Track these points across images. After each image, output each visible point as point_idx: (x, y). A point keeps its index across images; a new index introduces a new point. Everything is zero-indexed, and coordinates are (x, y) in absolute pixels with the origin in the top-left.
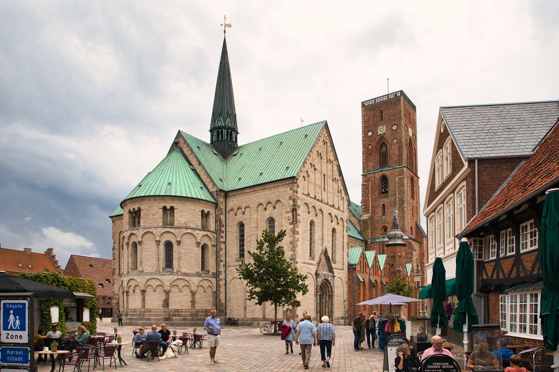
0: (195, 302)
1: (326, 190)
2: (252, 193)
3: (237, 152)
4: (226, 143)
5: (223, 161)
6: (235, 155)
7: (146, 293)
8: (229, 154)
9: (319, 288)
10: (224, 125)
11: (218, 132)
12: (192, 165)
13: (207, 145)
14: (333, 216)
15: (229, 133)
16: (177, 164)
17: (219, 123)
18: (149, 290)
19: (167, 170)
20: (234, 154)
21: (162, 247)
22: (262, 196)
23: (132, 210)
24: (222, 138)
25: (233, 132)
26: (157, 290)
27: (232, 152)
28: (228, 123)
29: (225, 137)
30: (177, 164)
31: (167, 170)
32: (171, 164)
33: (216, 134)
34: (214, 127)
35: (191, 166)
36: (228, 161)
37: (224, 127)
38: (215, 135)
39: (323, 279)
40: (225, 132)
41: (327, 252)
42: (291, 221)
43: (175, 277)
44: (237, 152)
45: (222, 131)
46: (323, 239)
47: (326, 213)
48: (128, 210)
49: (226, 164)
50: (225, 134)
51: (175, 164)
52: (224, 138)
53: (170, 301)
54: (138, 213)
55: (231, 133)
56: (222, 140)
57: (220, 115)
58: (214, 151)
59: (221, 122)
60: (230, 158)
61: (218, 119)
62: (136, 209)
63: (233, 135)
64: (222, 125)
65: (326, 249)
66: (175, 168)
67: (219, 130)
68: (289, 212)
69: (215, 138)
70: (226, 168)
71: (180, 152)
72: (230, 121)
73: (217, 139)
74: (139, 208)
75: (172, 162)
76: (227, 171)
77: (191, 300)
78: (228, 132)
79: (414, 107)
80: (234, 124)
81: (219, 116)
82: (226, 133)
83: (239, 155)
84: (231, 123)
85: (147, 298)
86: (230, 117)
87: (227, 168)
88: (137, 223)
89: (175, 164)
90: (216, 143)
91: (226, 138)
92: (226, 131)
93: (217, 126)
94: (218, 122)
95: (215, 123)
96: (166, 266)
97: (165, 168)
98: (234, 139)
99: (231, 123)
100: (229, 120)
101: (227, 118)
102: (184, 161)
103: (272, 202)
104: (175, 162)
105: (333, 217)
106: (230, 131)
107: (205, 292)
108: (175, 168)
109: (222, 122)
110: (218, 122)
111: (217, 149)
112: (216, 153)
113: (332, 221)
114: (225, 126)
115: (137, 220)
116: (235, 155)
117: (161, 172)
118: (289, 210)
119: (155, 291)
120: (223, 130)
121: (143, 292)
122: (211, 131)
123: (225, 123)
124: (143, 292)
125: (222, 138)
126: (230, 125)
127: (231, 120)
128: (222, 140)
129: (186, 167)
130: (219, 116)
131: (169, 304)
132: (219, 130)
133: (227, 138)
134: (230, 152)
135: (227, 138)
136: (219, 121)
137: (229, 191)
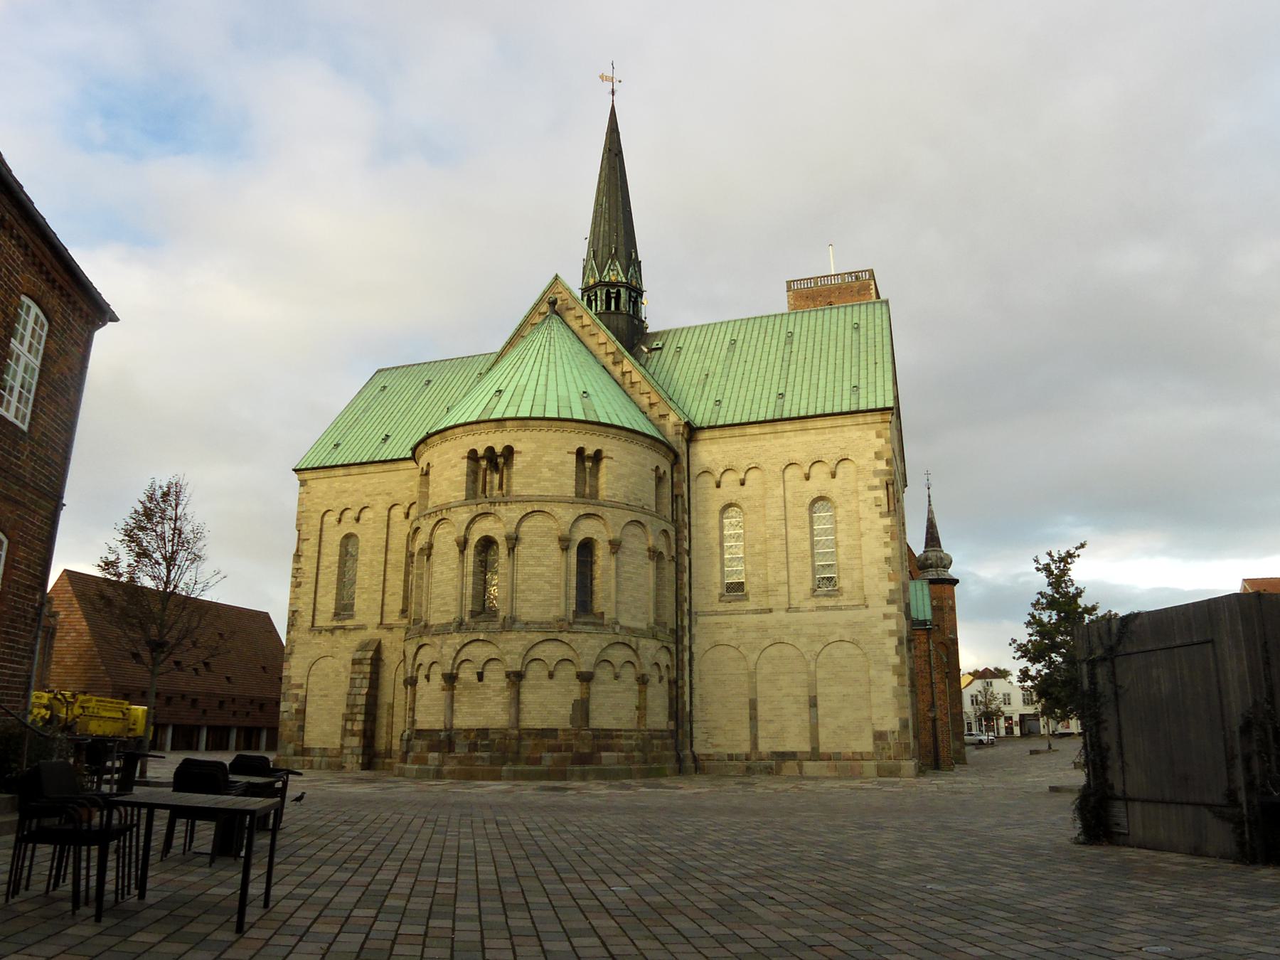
2: (768, 436)
7: (524, 682)
17: (611, 273)
18: (534, 671)
22: (797, 443)
26: (560, 674)
42: (885, 508)
53: (592, 707)
59: (615, 273)
64: (620, 279)
68: (876, 487)
85: (528, 696)
93: (607, 280)
94: (608, 272)
103: (827, 461)
109: (618, 273)
110: (608, 272)
118: (876, 482)
119: (551, 676)
120: (622, 290)
121: (516, 678)
124: (516, 678)
131: (591, 715)
132: (612, 291)
137: (702, 429)
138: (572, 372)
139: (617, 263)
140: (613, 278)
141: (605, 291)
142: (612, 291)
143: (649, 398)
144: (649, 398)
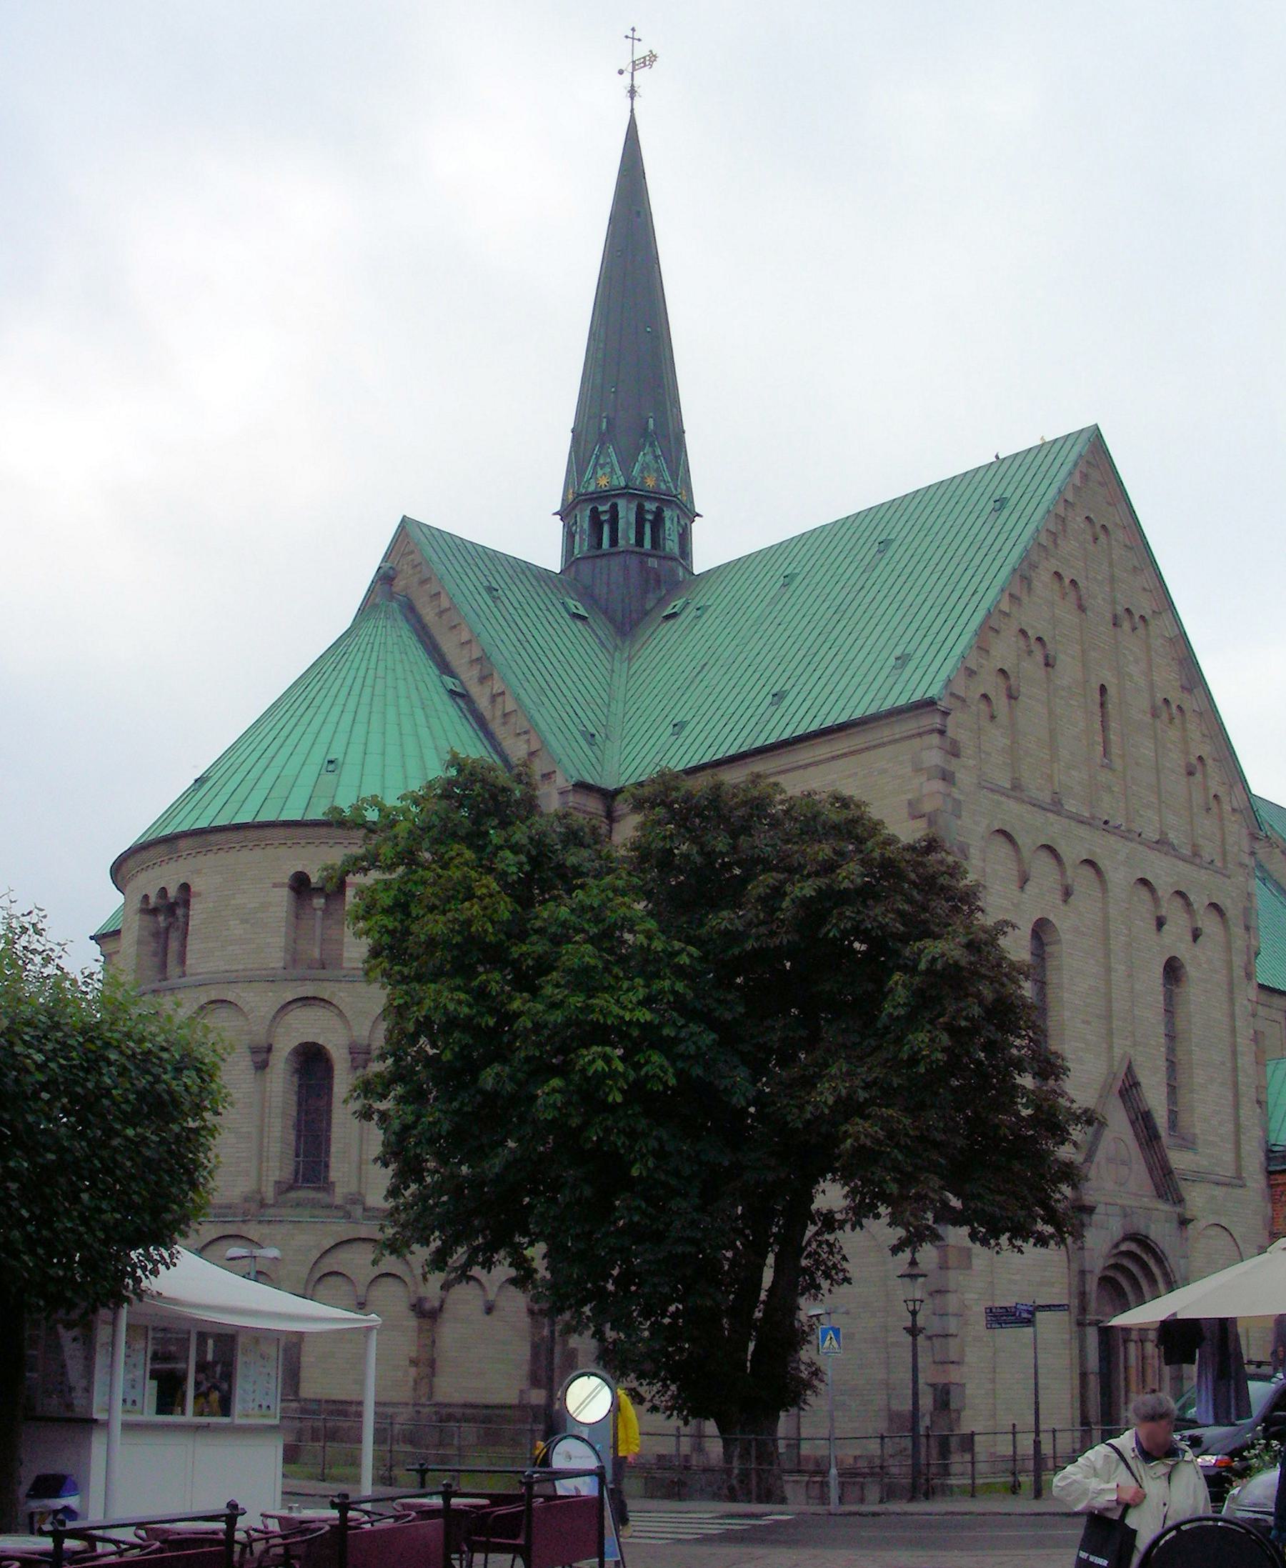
0: (432, 1364)
1: (1118, 764)
3: (680, 603)
4: (633, 562)
5: (616, 647)
6: (673, 616)
8: (646, 613)
9: (1092, 1285)
10: (623, 484)
11: (595, 514)
12: (452, 674)
13: (541, 575)
14: (1164, 892)
15: (650, 517)
16: (381, 673)
17: (600, 472)
19: (329, 700)
20: (669, 611)
21: (280, 1079)
23: (153, 900)
24: (614, 541)
25: (667, 514)
27: (662, 602)
28: (642, 471)
29: (628, 539)
30: (381, 673)
31: (329, 700)
32: (352, 672)
33: (586, 525)
34: (579, 495)
35: (448, 679)
36: (637, 647)
37: (627, 492)
38: (582, 531)
39: (1118, 1234)
40: (627, 513)
41: (1136, 1084)
43: (343, 1230)
44: (680, 603)
45: (614, 510)
46: (1108, 1016)
47: (1119, 877)
48: (140, 897)
49: (630, 659)
50: (628, 523)
51: (371, 672)
52: (621, 542)
54: (180, 912)
55: (659, 516)
56: (613, 550)
57: (603, 439)
58: (571, 603)
59: (608, 470)
60: (651, 630)
61: (598, 458)
62: (172, 893)
63: (668, 524)
64: (615, 482)
65: (1129, 1068)
66: (368, 690)
67: (601, 509)
69: (580, 547)
70: (623, 680)
71: (399, 617)
72: (653, 465)
73: (591, 547)
74: (185, 888)
75: (355, 665)
76: (629, 695)
77: (414, 1355)
78: (640, 511)
80: (674, 474)
81: (603, 444)
82: (632, 518)
83: (691, 612)
84: (658, 470)
86: (652, 445)
87: (629, 678)
88: (173, 969)
89: (371, 672)
90: (585, 568)
91: (633, 541)
92: (634, 506)
93: (592, 488)
94: (594, 472)
95: (581, 473)
96: (297, 1172)
97: (323, 692)
98: (672, 545)
99: (658, 470)
100: (649, 458)
101: (642, 448)
102: (418, 654)
104: (372, 665)
105: (1164, 903)
106: (651, 506)
107: (489, 1309)
108: (368, 690)
109: (613, 470)
110: (594, 472)
111: (587, 595)
112: (582, 612)
113: (1160, 923)
114: (626, 487)
115: (174, 945)
116: (673, 616)
117: (299, 713)
120: (622, 504)
122: (566, 513)
123: (628, 479)
125: (614, 541)
126: (650, 483)
127: (656, 457)
128: (613, 550)
129: (421, 685)
130: (603, 444)
131: (304, 1374)
133: (640, 542)
134: (649, 605)
135: (640, 542)
136: (602, 466)
138: (412, 714)
139: (611, 449)
140: (603, 482)
141: (588, 512)
142: (601, 509)
143: (528, 741)
144: (528, 741)
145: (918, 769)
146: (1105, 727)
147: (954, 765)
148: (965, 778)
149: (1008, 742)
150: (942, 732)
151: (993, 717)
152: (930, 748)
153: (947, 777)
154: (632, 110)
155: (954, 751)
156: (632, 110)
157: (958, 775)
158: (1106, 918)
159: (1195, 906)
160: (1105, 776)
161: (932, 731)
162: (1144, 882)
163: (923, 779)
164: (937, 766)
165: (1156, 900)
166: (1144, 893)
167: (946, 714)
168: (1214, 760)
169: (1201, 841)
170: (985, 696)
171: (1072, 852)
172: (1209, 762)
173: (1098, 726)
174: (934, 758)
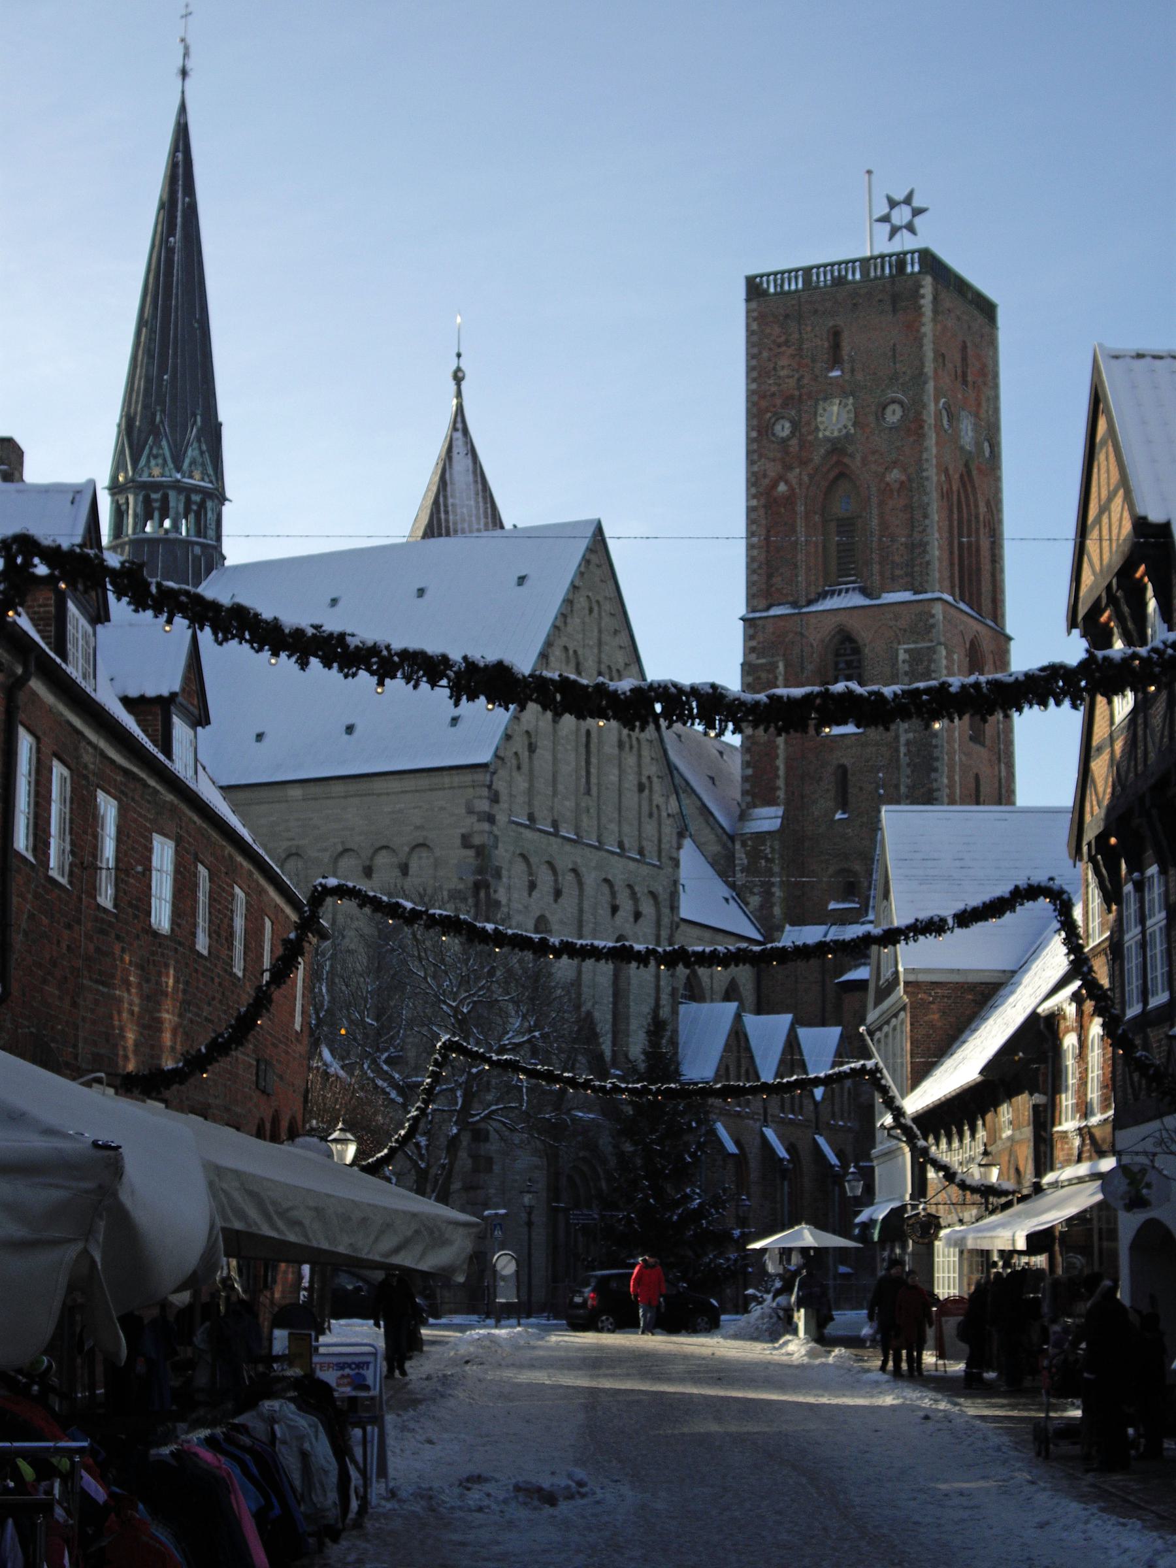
47: (591, 879)
79: (986, 309)
145: (470, 811)
146: (588, 762)
147: (495, 810)
148: (501, 818)
149: (526, 785)
150: (490, 787)
151: (519, 768)
152: (480, 797)
153: (491, 819)
154: (183, 92)
155: (495, 799)
156: (183, 92)
157: (498, 817)
158: (581, 911)
159: (639, 895)
160: (585, 802)
161: (484, 785)
162: (606, 880)
163: (474, 818)
164: (485, 812)
165: (613, 894)
166: (605, 889)
167: (494, 773)
168: (658, 777)
169: (645, 843)
170: (516, 753)
171: (563, 864)
172: (655, 780)
173: (583, 764)
174: (484, 806)
